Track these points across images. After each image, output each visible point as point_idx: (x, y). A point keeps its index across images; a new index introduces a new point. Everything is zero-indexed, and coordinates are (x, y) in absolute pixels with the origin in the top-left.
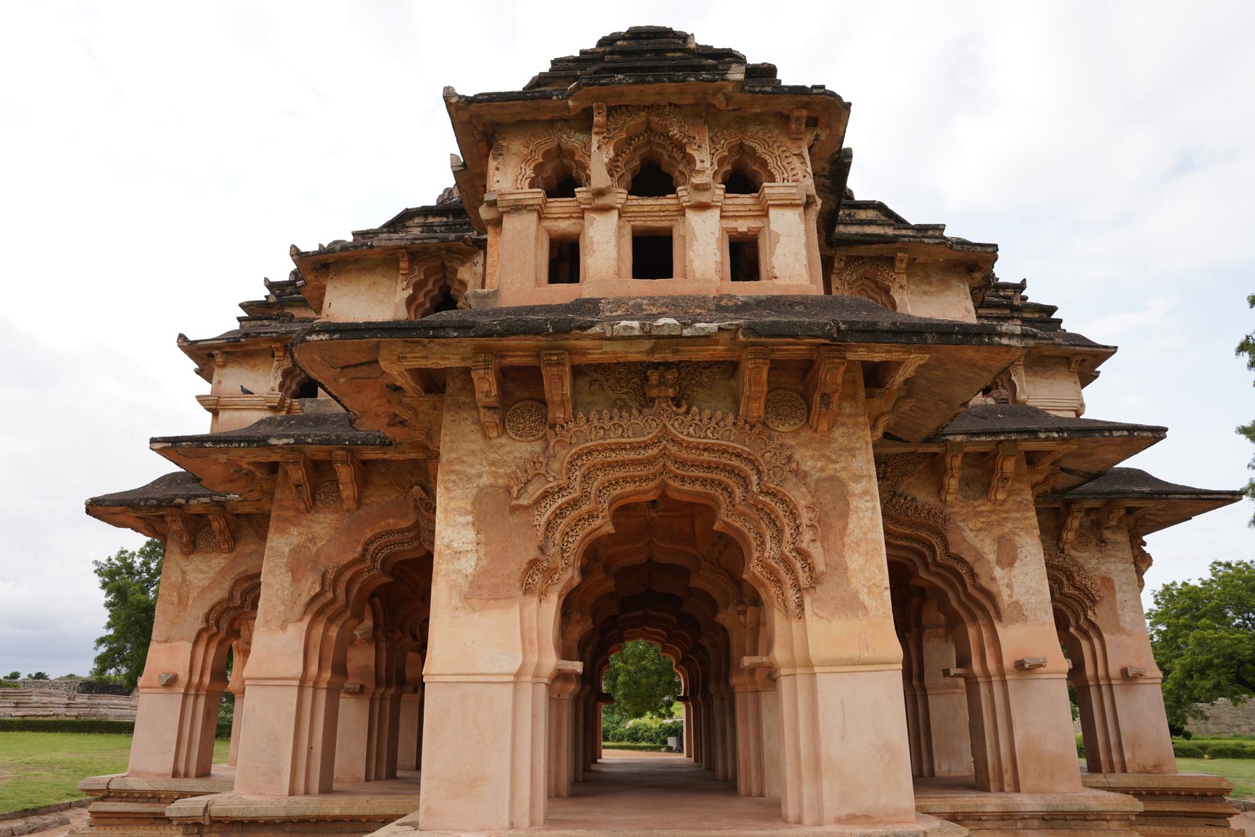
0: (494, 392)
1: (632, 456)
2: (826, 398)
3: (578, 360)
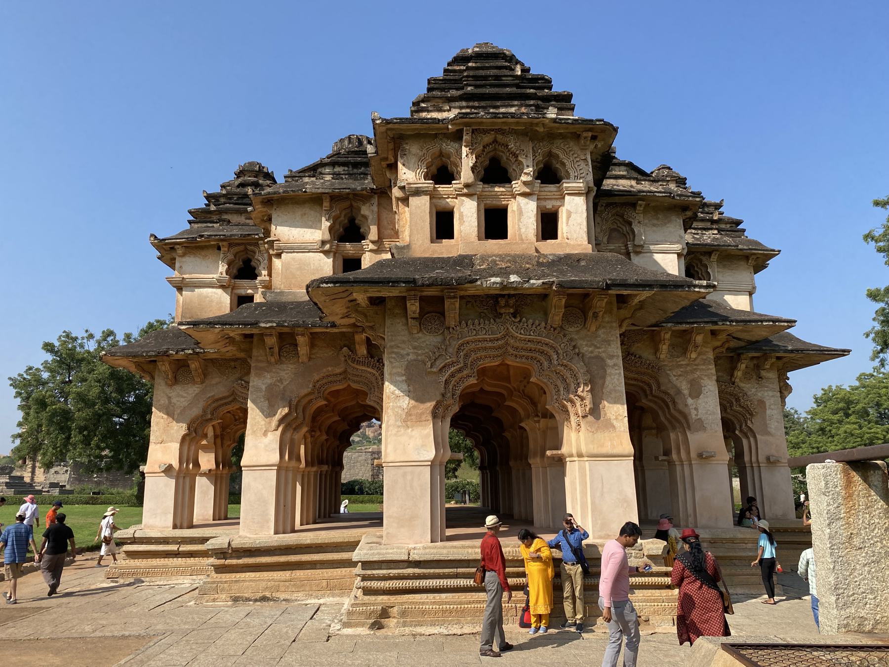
0: (418, 311)
1: (490, 344)
2: (595, 315)
3: (462, 293)
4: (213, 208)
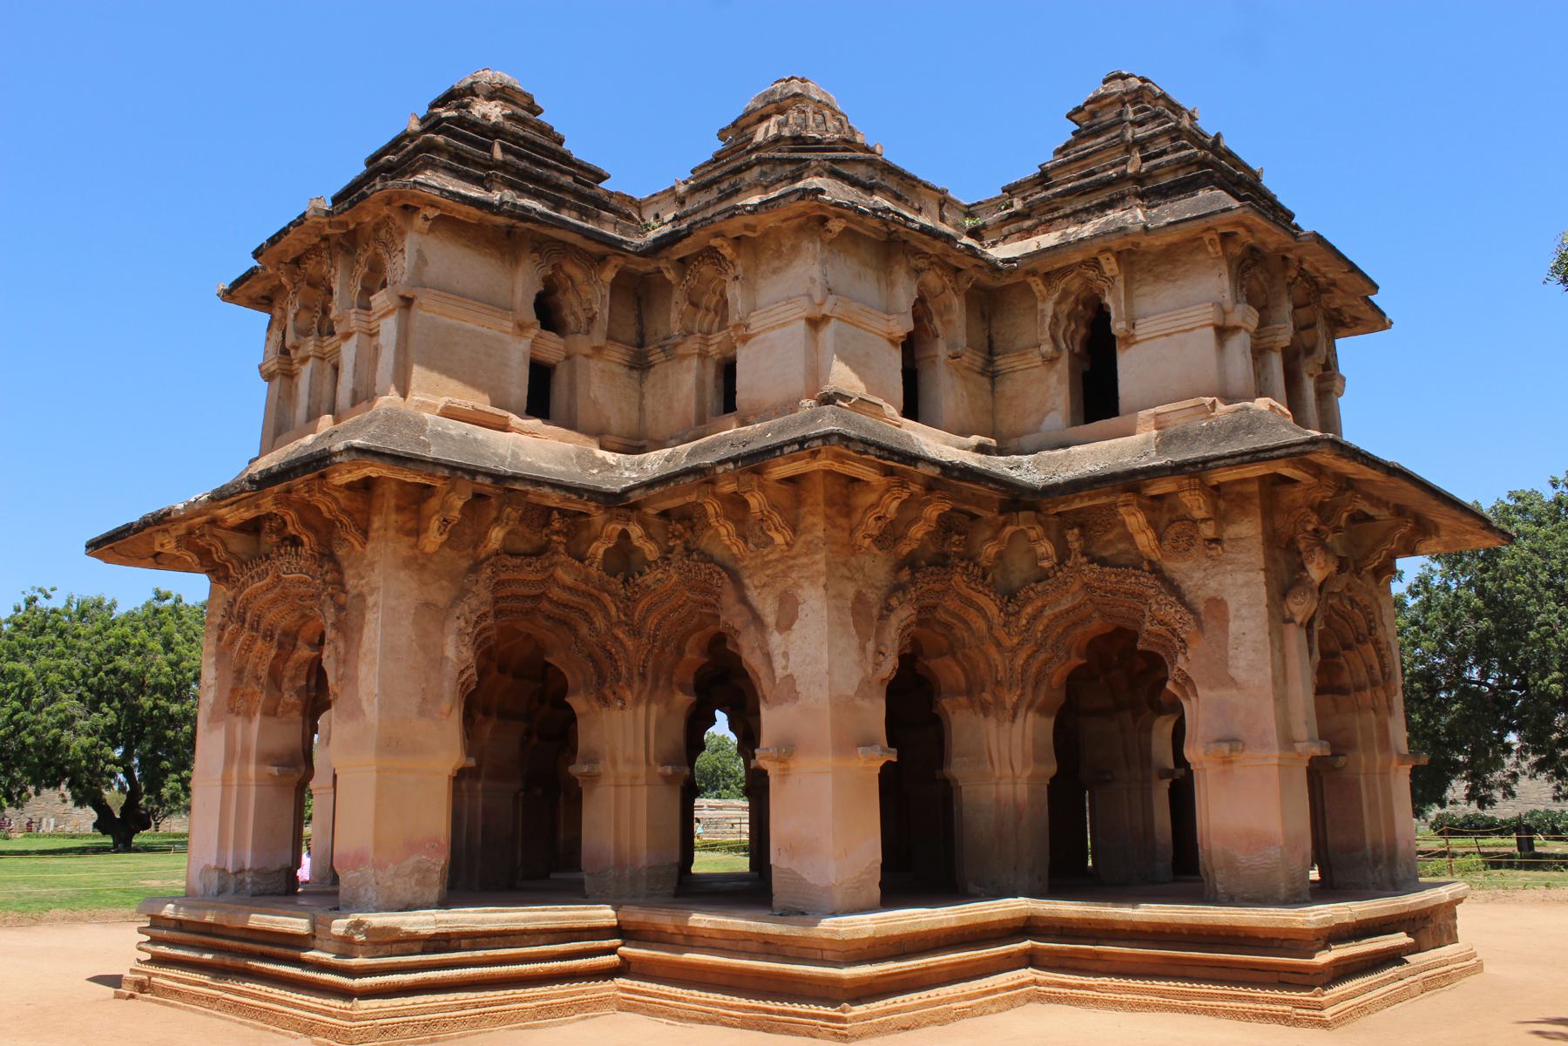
1: (270, 596)
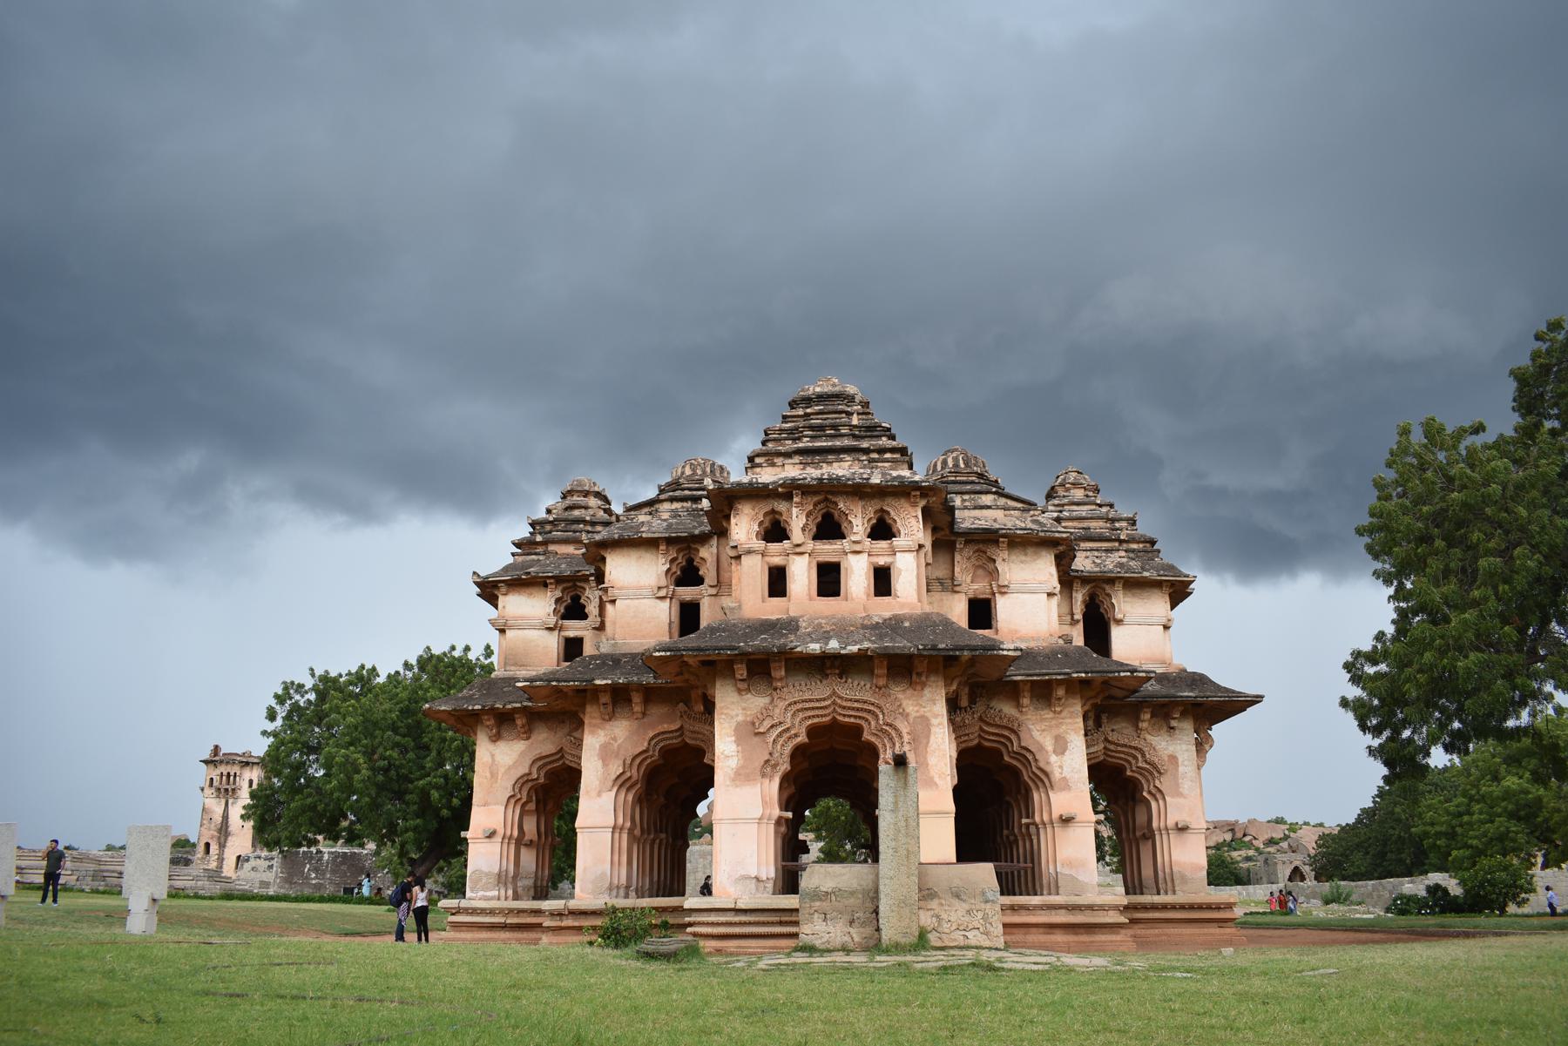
4: (539, 538)
